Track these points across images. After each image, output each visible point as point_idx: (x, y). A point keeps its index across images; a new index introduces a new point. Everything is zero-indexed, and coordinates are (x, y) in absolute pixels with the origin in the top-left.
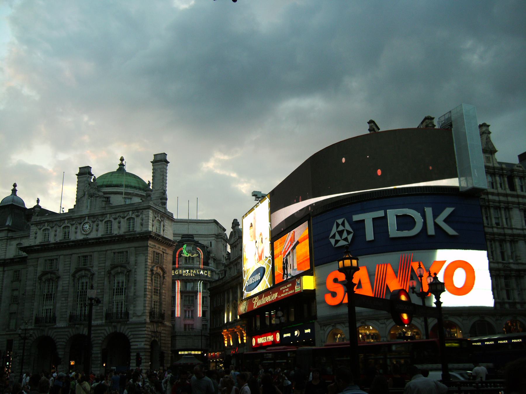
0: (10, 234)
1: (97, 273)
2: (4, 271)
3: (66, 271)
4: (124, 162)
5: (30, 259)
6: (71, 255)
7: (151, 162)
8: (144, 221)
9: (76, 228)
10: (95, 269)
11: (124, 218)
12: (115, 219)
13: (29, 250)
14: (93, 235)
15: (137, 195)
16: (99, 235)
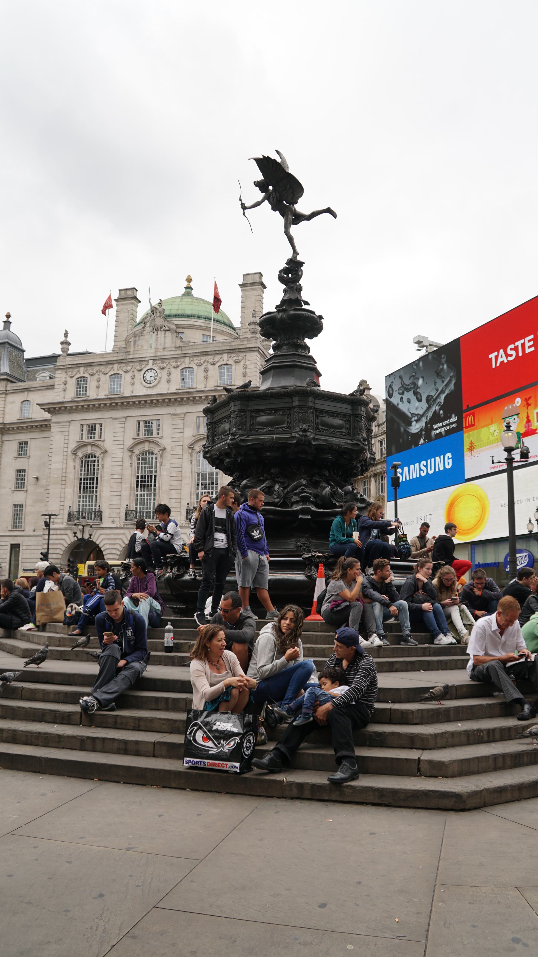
0: (10, 386)
1: (168, 448)
3: (117, 443)
4: (192, 284)
5: (55, 423)
6: (126, 418)
7: (240, 285)
8: (248, 370)
9: (133, 377)
10: (166, 442)
11: (213, 364)
12: (199, 365)
13: (54, 409)
14: (162, 389)
15: (222, 333)
16: (173, 390)
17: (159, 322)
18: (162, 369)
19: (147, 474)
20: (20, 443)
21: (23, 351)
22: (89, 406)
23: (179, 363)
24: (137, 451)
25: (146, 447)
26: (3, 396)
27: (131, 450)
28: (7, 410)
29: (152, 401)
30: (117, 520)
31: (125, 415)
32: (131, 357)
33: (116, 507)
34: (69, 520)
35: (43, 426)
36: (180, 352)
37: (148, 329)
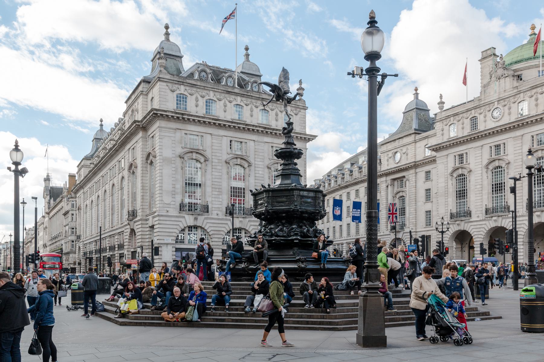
0: (418, 137)
2: (416, 173)
9: (485, 117)
14: (506, 120)
16: (513, 120)
17: (500, 72)
18: (505, 106)
19: (498, 182)
20: (426, 172)
21: (428, 110)
22: (457, 142)
23: (516, 99)
24: (491, 167)
25: (497, 163)
26: (414, 144)
27: (487, 167)
28: (417, 153)
29: (497, 131)
30: (480, 215)
31: (482, 144)
32: (482, 102)
33: (480, 206)
34: (451, 218)
35: (433, 161)
36: (516, 91)
37: (493, 79)
